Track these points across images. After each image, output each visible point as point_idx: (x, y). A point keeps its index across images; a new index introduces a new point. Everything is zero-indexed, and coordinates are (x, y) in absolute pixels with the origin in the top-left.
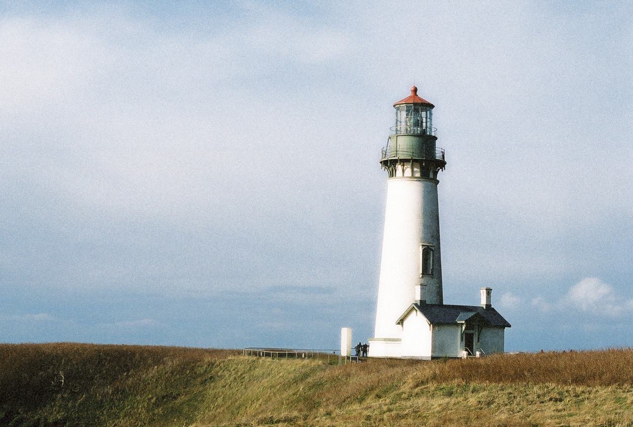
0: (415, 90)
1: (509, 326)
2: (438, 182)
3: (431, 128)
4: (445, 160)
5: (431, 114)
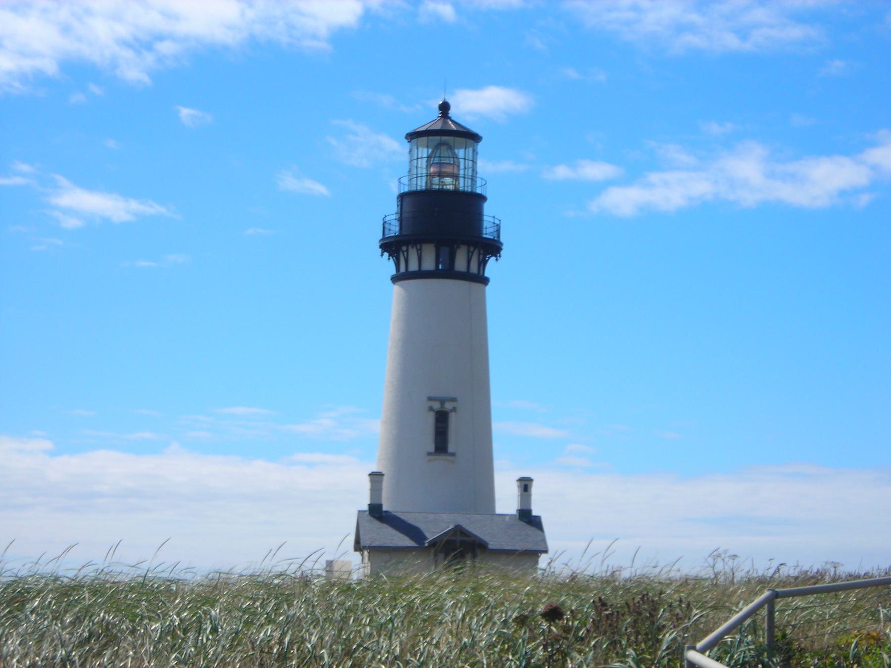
0: (445, 108)
2: (485, 281)
3: (473, 179)
4: (502, 240)
5: (475, 152)
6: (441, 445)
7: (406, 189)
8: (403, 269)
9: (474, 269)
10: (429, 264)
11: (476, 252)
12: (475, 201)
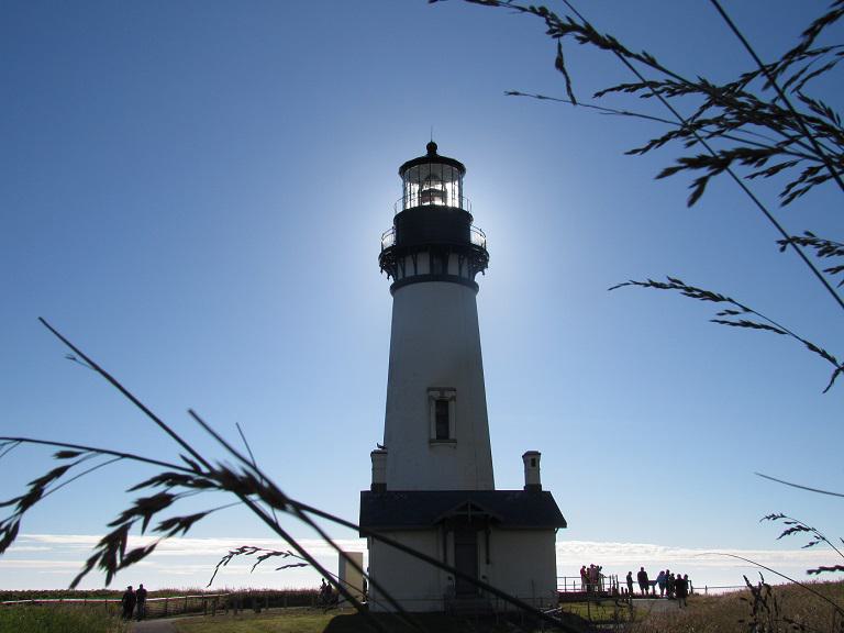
0: (432, 147)
1: (564, 524)
6: (443, 435)
7: (400, 210)
8: (400, 277)
9: (465, 274)
10: (424, 268)
11: (466, 260)
12: (462, 219)
